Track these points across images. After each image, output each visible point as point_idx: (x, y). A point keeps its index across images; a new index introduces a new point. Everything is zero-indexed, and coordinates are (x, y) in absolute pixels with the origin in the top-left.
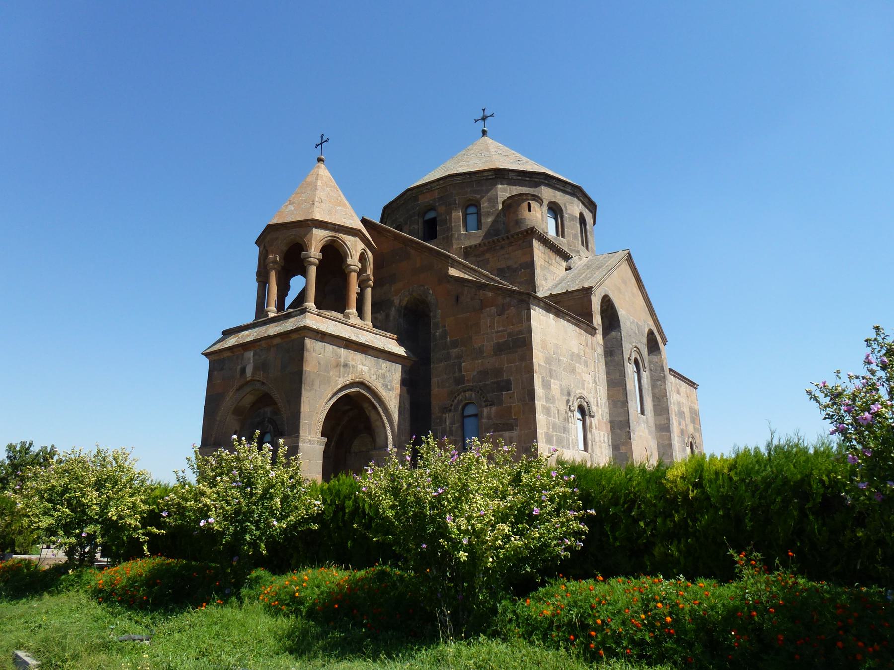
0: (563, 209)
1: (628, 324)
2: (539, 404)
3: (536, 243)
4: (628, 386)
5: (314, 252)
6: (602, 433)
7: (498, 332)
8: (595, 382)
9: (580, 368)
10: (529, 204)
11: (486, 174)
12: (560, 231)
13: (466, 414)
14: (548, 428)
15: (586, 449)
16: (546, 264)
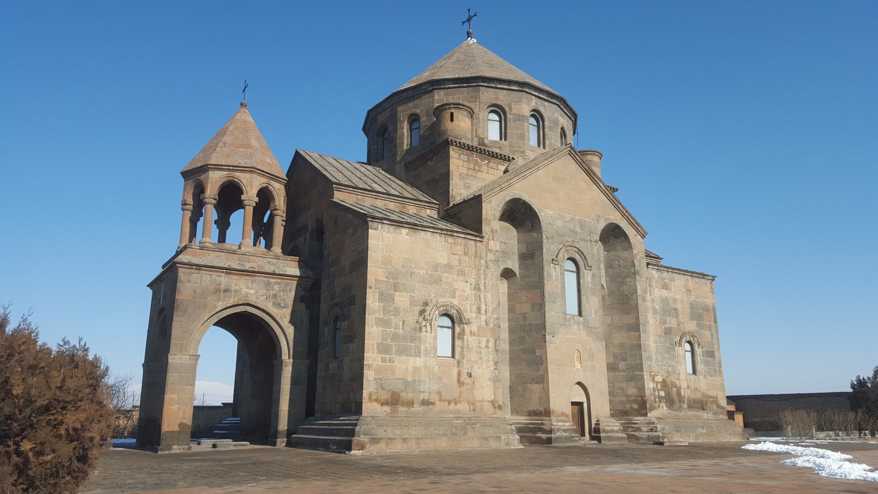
0: (507, 109)
1: (560, 223)
2: (370, 318)
3: (453, 153)
4: (548, 287)
5: (211, 192)
6: (484, 340)
7: (353, 251)
8: (477, 288)
9: (447, 277)
10: (452, 114)
11: (424, 87)
12: (503, 135)
13: (338, 326)
14: (383, 339)
15: (453, 356)
16: (471, 172)
